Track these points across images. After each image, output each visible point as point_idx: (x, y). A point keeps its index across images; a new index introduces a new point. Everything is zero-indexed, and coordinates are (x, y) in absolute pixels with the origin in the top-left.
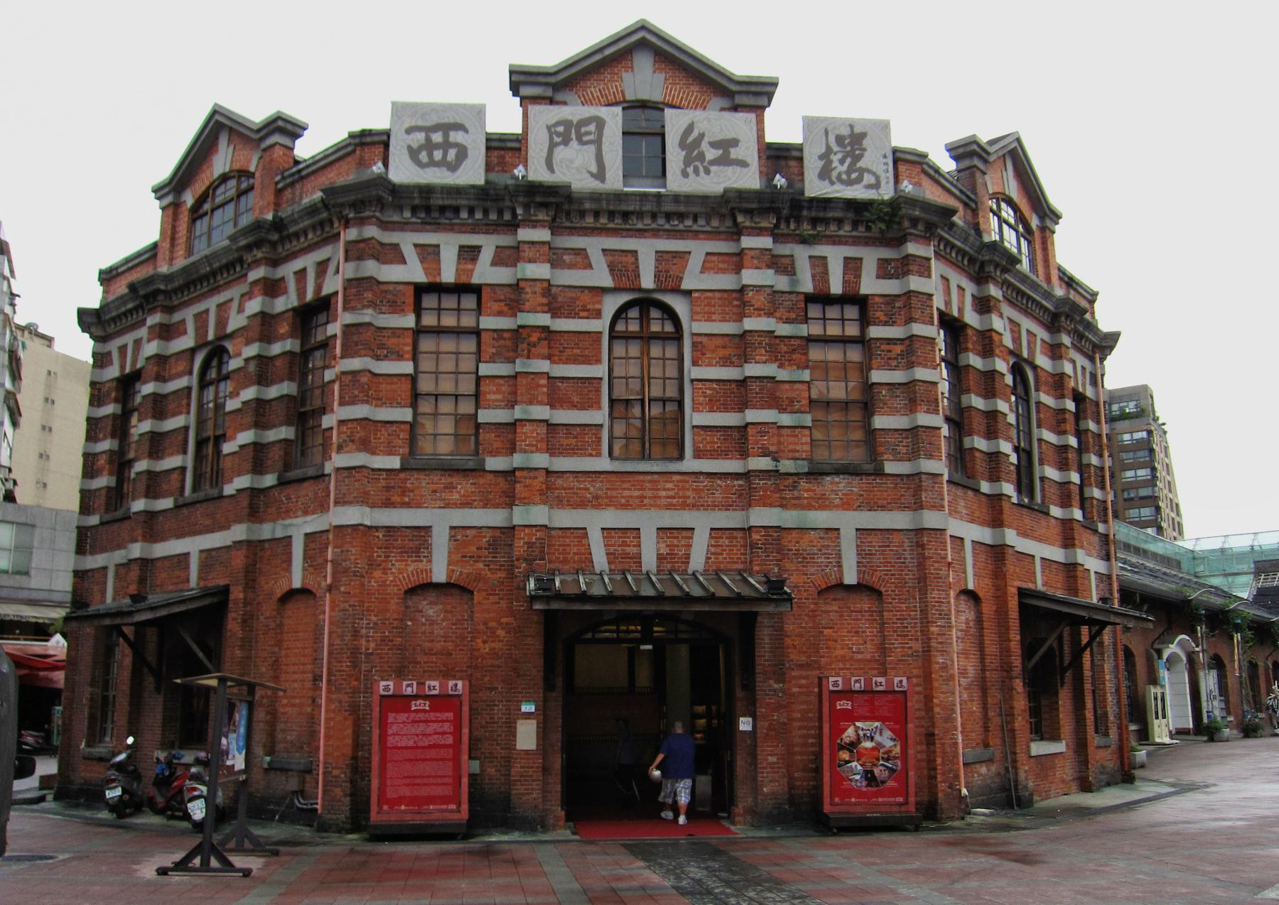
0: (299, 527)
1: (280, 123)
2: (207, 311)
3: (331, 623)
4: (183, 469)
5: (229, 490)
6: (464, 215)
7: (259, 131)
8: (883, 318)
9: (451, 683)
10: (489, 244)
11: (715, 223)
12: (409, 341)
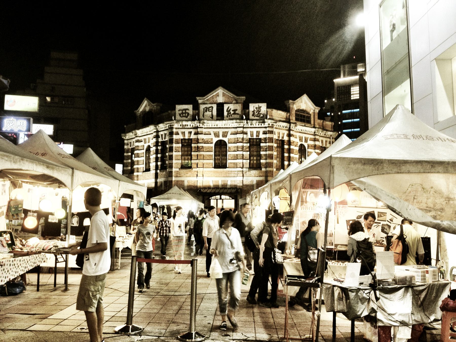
6: (189, 125)
8: (263, 141)
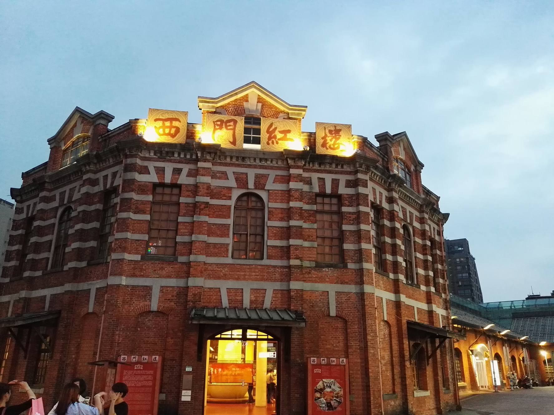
0: (94, 285)
1: (102, 115)
2: (65, 191)
3: (103, 328)
4: (48, 259)
5: (66, 268)
6: (176, 155)
7: (92, 118)
8: (348, 204)
9: (153, 357)
10: (186, 168)
11: (280, 163)
12: (149, 206)
